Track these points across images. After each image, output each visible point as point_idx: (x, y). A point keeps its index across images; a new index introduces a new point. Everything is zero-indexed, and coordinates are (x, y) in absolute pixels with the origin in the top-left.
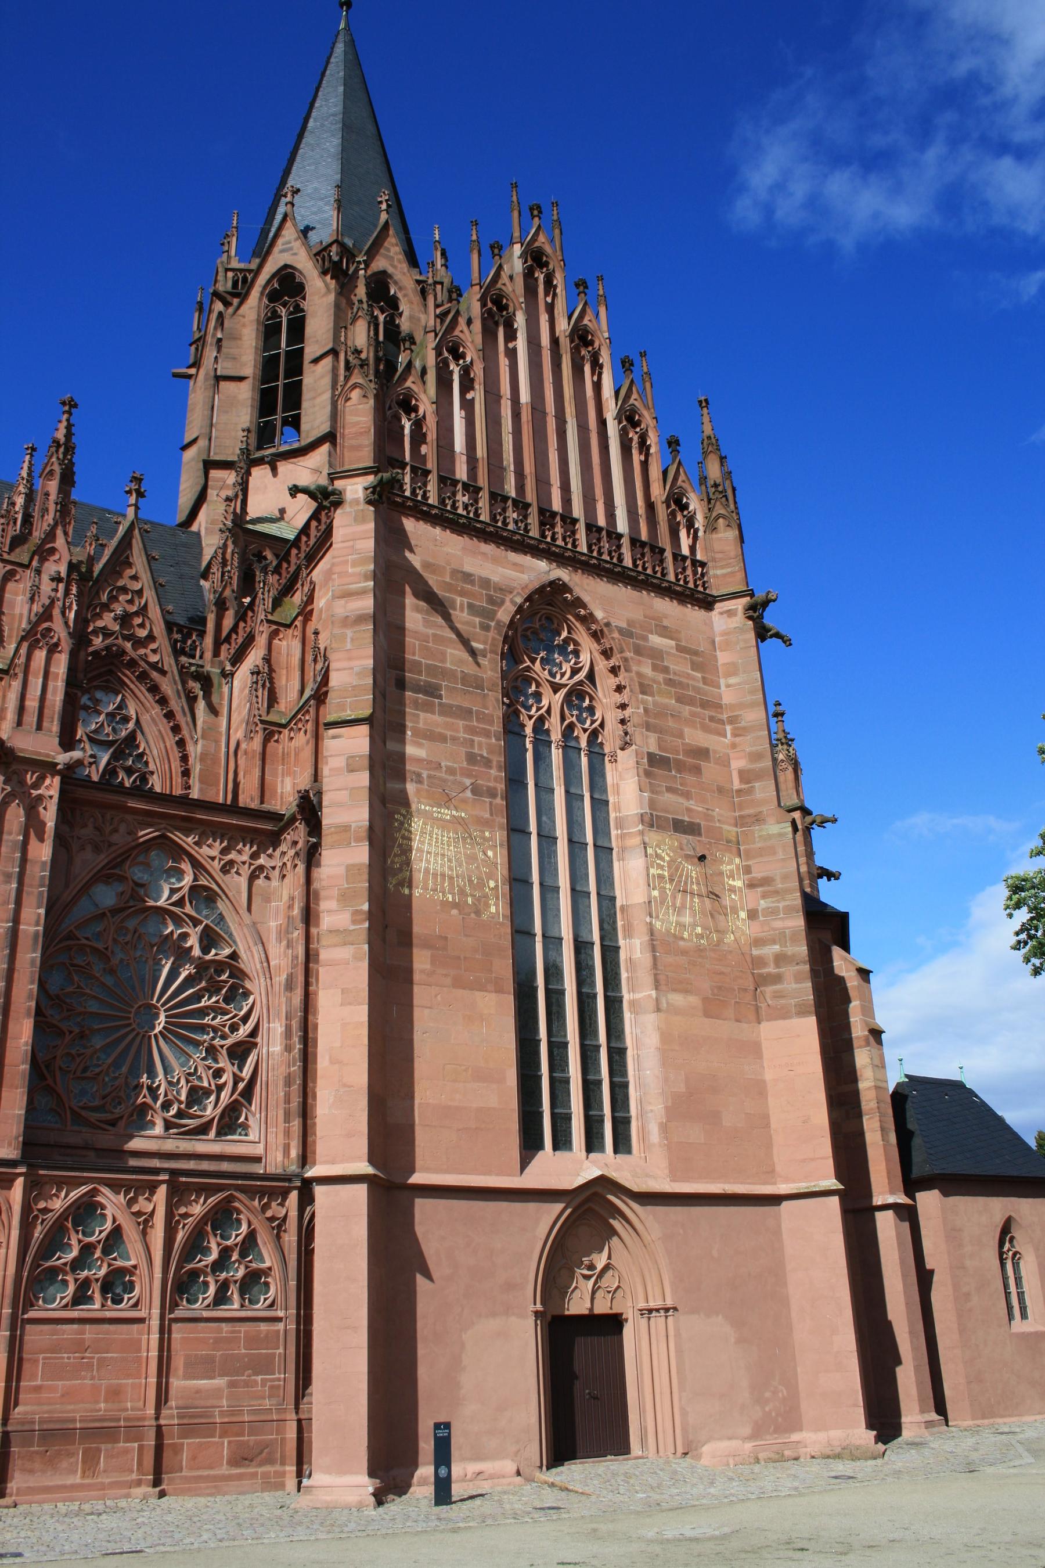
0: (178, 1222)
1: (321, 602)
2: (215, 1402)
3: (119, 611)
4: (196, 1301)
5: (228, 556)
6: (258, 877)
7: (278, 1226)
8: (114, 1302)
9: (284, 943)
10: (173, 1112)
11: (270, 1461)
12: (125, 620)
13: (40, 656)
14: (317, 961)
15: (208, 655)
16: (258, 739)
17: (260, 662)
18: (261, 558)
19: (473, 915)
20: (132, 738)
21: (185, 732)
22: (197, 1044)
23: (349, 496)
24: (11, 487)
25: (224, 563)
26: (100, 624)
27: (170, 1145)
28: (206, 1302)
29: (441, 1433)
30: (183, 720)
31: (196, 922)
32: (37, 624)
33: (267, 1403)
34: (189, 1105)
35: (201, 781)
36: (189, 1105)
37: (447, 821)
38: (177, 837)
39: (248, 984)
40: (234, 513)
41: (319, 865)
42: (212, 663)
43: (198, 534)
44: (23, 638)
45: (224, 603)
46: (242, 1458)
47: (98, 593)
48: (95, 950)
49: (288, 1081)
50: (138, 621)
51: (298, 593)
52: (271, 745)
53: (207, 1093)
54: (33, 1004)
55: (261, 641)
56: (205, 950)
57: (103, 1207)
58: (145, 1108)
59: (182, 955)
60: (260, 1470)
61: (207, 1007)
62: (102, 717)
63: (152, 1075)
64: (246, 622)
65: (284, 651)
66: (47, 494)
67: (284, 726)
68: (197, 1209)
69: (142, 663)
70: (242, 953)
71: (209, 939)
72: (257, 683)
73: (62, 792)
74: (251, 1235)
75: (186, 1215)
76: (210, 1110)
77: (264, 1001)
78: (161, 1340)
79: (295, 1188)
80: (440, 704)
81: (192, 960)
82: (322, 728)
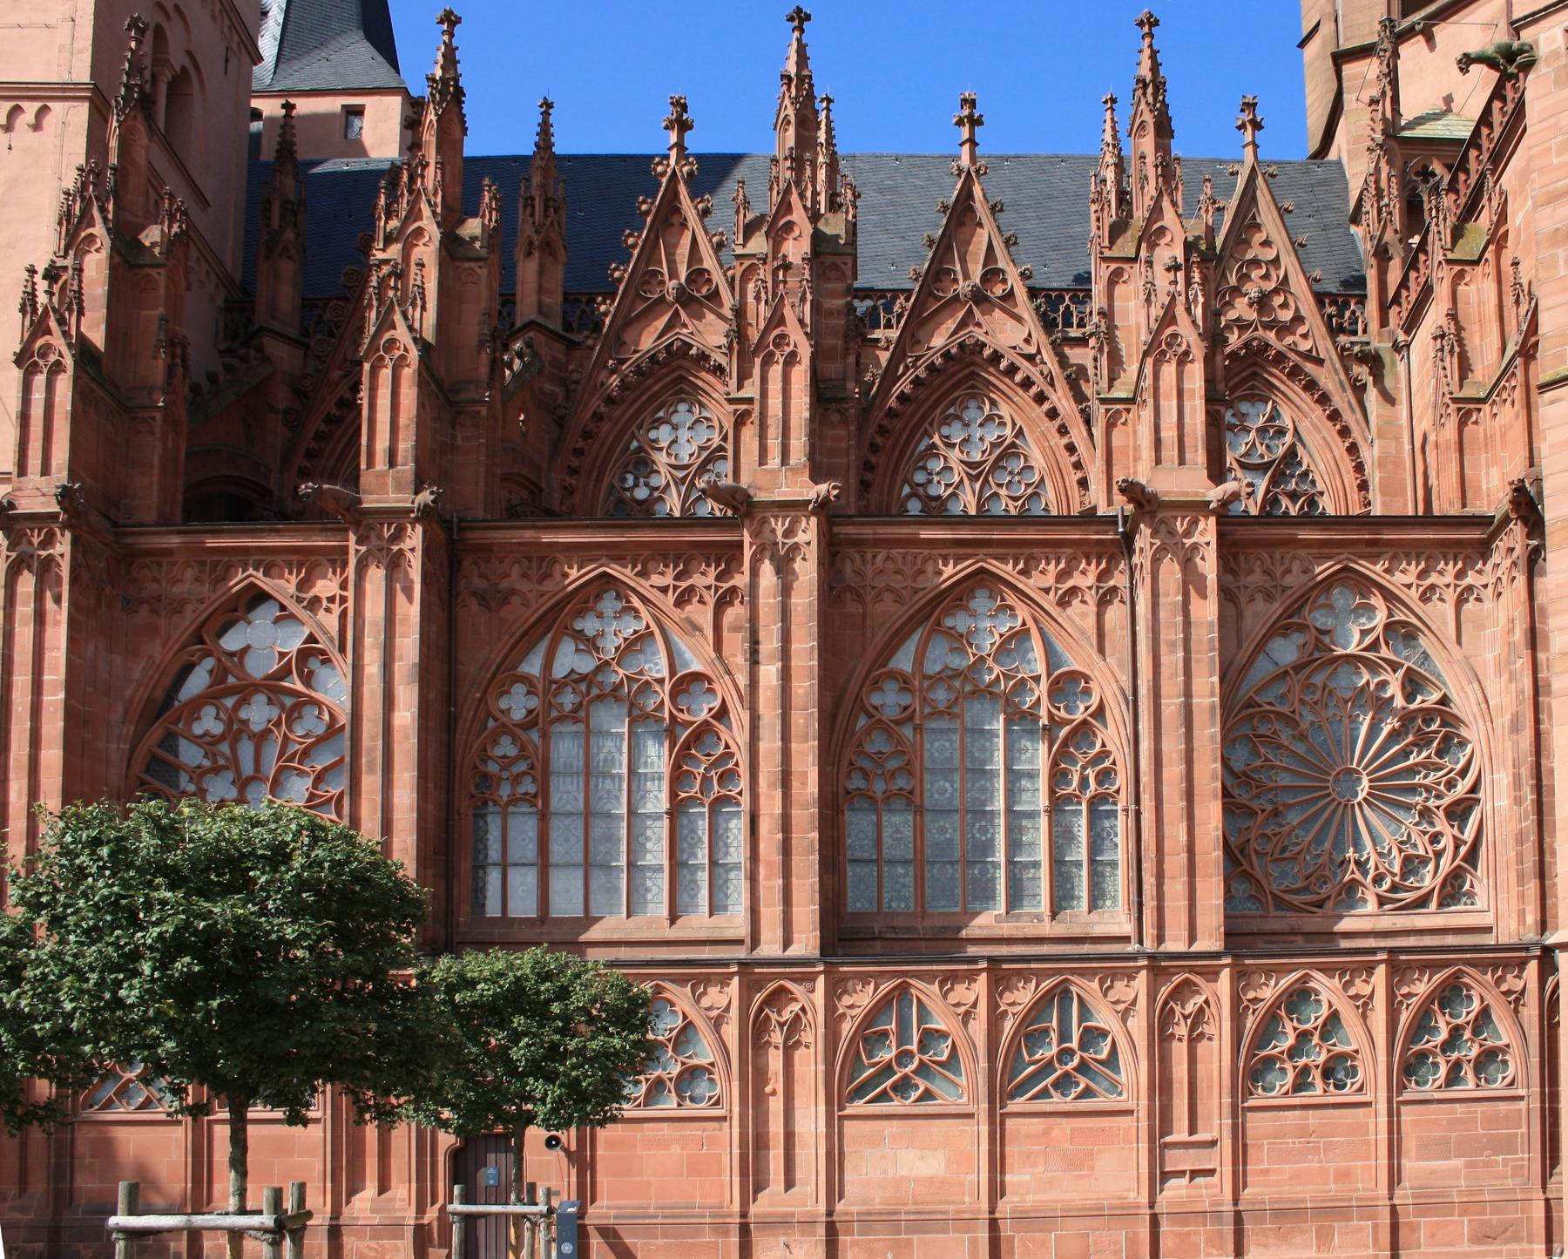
0: (1401, 1002)
1: (1516, 220)
2: (1451, 1183)
3: (1254, 294)
4: (1426, 1083)
5: (1383, 184)
6: (1467, 600)
7: (1516, 1000)
8: (1337, 1087)
9: (1505, 676)
10: (1386, 885)
11: (1516, 1239)
12: (1262, 302)
13: (1169, 370)
14: (1549, 693)
15: (1374, 325)
16: (1452, 424)
17: (1443, 321)
18: (1426, 174)
20: (1291, 453)
21: (1356, 434)
22: (1408, 807)
23: (1543, 50)
24: (1096, 161)
25: (1379, 195)
26: (1232, 315)
27: (1387, 922)
28: (1437, 1084)
30: (1351, 418)
31: (1395, 667)
32: (1159, 331)
33: (1510, 1183)
34: (1404, 877)
35: (1383, 493)
36: (1404, 877)
38: (1363, 566)
39: (1464, 732)
40: (1384, 119)
41: (1543, 573)
42: (1380, 335)
43: (1339, 163)
44: (1146, 354)
45: (1386, 251)
46: (1484, 1236)
47: (1224, 275)
48: (1280, 715)
49: (1520, 839)
50: (1278, 300)
51: (1485, 213)
52: (1469, 429)
53: (1424, 861)
54: (1219, 785)
55: (1442, 291)
56: (1409, 698)
57: (1317, 993)
58: (1353, 885)
59: (1383, 707)
60: (1504, 1248)
61: (1416, 764)
62: (1253, 433)
63: (1358, 846)
64: (1417, 270)
65: (1473, 299)
66: (1143, 157)
67: (1483, 401)
68: (1422, 987)
69: (1292, 355)
70: (1453, 696)
71: (1413, 685)
72: (1442, 349)
73: (1220, 535)
74: (1485, 1013)
75: (1409, 995)
76: (1429, 880)
77: (1485, 750)
78: (1390, 1123)
79: (1533, 957)
81: (1393, 712)
82: (1534, 392)
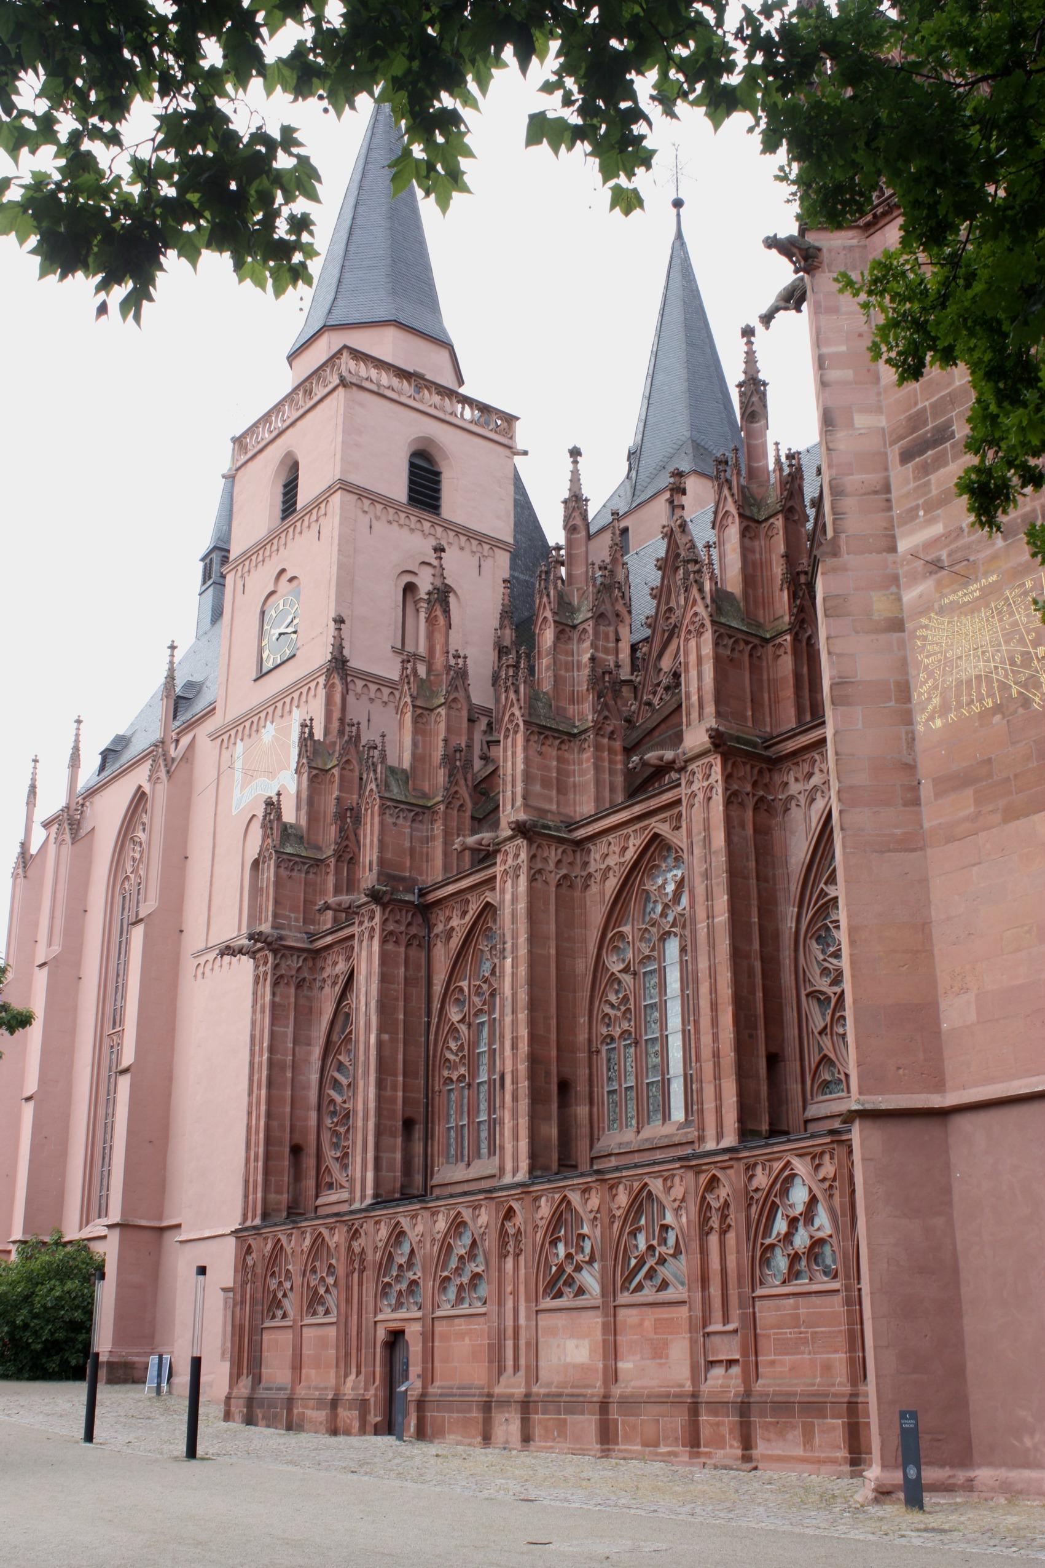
19: (1021, 711)
29: (909, 1424)
37: (978, 598)
80: (953, 446)
